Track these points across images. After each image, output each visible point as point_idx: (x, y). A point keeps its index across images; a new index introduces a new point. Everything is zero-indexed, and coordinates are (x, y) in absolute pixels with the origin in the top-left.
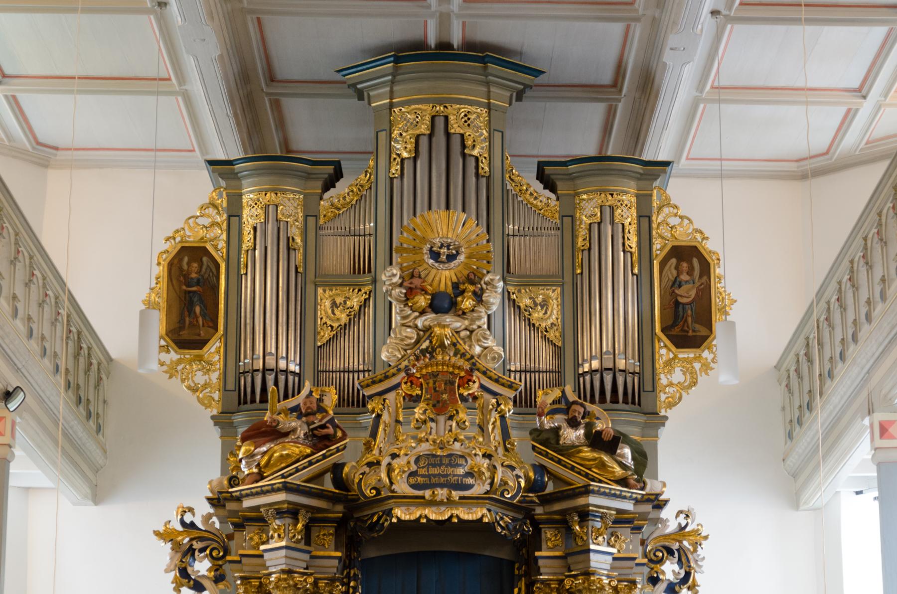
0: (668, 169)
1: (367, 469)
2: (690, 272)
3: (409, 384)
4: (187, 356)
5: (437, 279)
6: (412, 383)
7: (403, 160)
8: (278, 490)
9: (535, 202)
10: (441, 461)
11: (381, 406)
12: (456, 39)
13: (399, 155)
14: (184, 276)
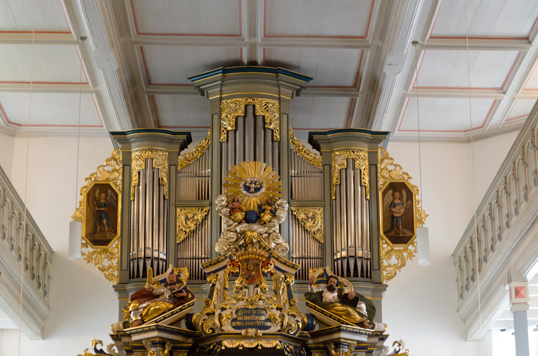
0: (387, 136)
1: (207, 317)
2: (401, 198)
3: (232, 266)
4: (99, 250)
5: (249, 202)
6: (234, 265)
7: (228, 131)
8: (153, 330)
9: (307, 156)
10: (251, 312)
11: (215, 279)
12: (260, 59)
13: (226, 129)
14: (97, 201)
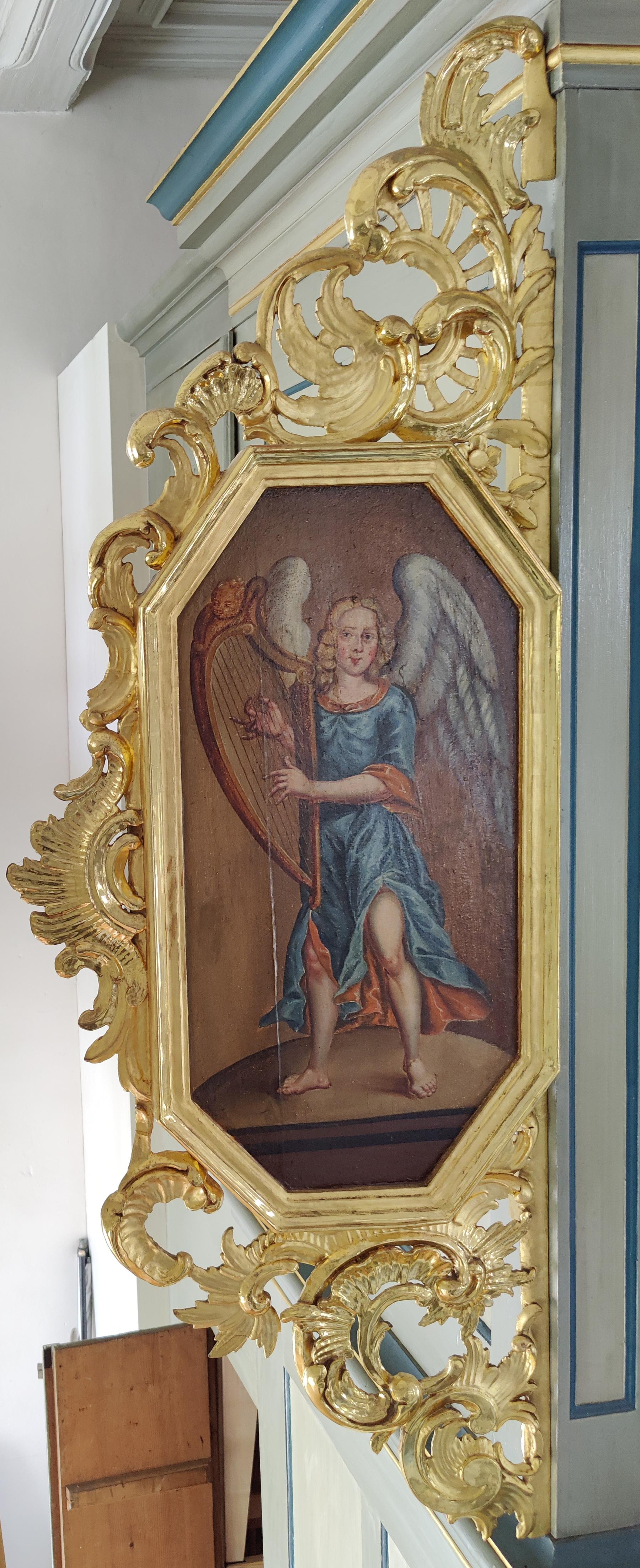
14: (293, 701)
